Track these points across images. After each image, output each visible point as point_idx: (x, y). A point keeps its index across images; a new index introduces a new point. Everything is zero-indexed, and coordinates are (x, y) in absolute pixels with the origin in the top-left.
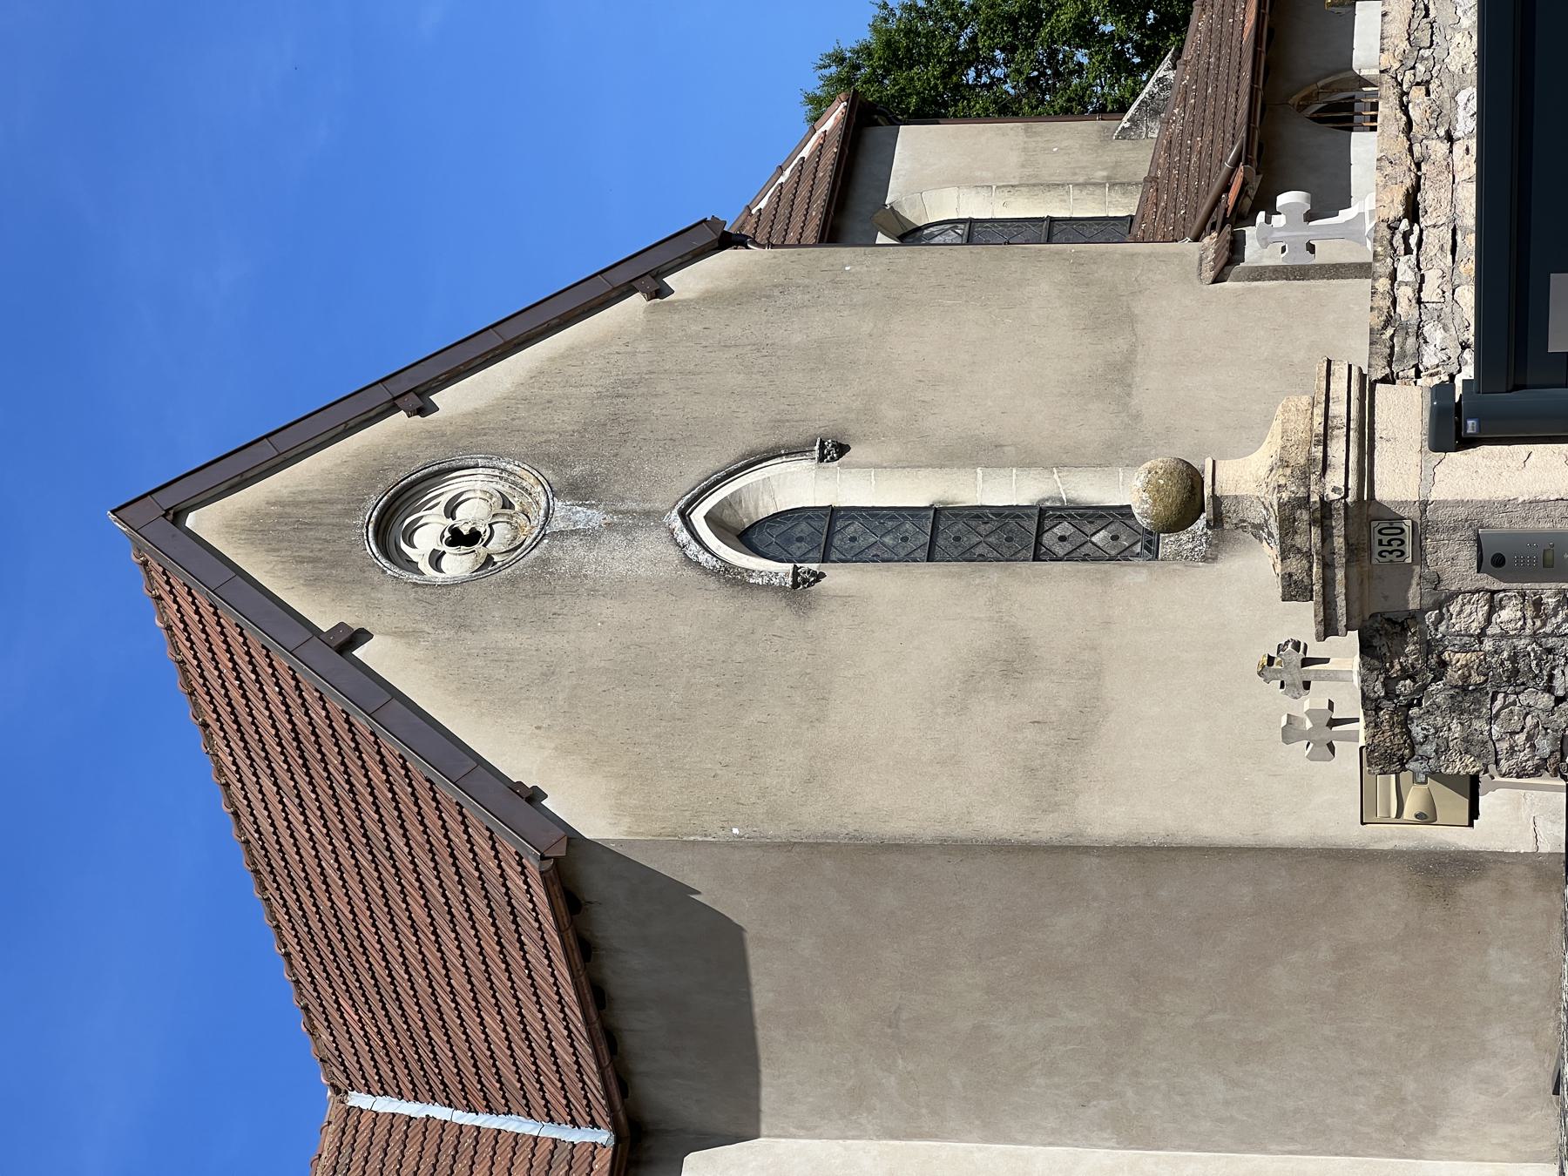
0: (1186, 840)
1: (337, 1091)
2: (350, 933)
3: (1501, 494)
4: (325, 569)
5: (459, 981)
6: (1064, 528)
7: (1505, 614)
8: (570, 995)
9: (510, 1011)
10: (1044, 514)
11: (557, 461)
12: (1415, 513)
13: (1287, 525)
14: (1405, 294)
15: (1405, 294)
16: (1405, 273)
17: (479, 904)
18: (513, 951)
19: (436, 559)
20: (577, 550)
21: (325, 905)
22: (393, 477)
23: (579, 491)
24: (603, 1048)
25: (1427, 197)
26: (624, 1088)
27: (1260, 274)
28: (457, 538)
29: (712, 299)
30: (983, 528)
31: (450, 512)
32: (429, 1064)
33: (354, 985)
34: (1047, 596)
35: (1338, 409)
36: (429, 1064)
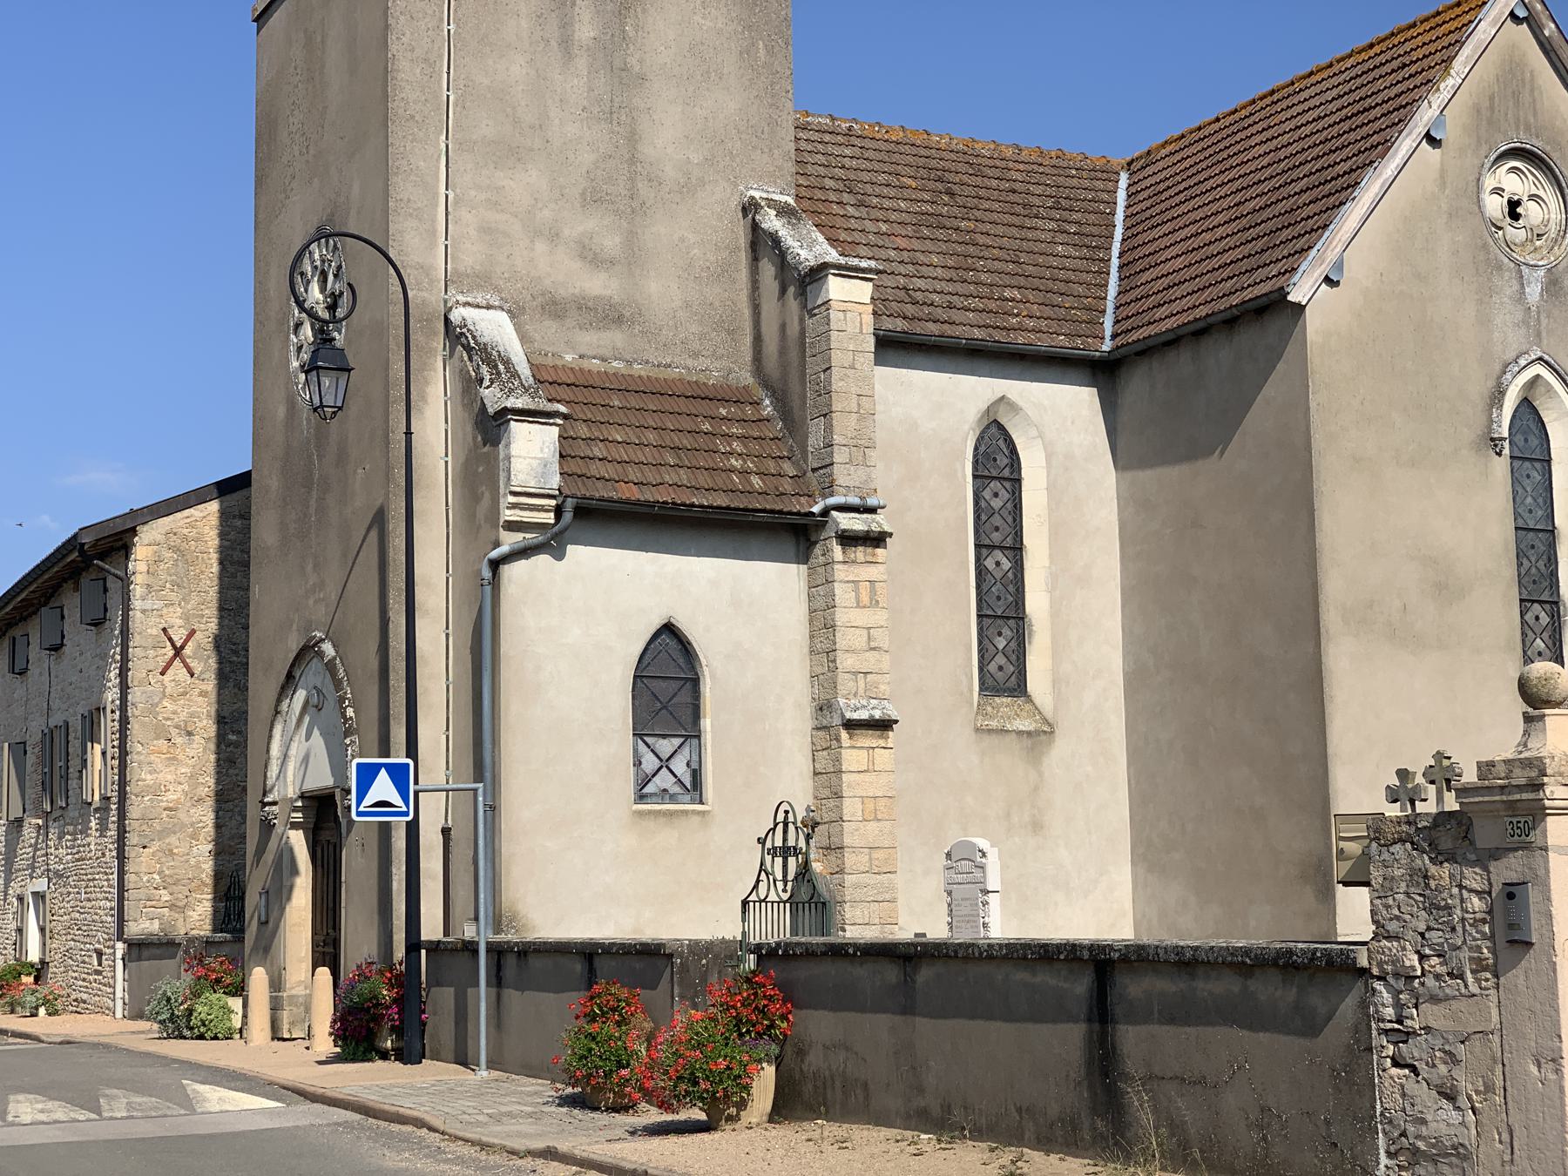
0: (1330, 709)
1: (1129, 164)
3: (1554, 896)
4: (1486, 115)
5: (1207, 237)
6: (1545, 619)
7: (1475, 900)
8: (1202, 312)
9: (1186, 274)
12: (1539, 843)
13: (1528, 763)
17: (1260, 244)
19: (1498, 191)
20: (1511, 288)
22: (1555, 156)
23: (1552, 284)
26: (1141, 354)
28: (1513, 207)
30: (1541, 564)
31: (1533, 197)
32: (1149, 224)
33: (1200, 167)
34: (1496, 609)
36: (1149, 224)
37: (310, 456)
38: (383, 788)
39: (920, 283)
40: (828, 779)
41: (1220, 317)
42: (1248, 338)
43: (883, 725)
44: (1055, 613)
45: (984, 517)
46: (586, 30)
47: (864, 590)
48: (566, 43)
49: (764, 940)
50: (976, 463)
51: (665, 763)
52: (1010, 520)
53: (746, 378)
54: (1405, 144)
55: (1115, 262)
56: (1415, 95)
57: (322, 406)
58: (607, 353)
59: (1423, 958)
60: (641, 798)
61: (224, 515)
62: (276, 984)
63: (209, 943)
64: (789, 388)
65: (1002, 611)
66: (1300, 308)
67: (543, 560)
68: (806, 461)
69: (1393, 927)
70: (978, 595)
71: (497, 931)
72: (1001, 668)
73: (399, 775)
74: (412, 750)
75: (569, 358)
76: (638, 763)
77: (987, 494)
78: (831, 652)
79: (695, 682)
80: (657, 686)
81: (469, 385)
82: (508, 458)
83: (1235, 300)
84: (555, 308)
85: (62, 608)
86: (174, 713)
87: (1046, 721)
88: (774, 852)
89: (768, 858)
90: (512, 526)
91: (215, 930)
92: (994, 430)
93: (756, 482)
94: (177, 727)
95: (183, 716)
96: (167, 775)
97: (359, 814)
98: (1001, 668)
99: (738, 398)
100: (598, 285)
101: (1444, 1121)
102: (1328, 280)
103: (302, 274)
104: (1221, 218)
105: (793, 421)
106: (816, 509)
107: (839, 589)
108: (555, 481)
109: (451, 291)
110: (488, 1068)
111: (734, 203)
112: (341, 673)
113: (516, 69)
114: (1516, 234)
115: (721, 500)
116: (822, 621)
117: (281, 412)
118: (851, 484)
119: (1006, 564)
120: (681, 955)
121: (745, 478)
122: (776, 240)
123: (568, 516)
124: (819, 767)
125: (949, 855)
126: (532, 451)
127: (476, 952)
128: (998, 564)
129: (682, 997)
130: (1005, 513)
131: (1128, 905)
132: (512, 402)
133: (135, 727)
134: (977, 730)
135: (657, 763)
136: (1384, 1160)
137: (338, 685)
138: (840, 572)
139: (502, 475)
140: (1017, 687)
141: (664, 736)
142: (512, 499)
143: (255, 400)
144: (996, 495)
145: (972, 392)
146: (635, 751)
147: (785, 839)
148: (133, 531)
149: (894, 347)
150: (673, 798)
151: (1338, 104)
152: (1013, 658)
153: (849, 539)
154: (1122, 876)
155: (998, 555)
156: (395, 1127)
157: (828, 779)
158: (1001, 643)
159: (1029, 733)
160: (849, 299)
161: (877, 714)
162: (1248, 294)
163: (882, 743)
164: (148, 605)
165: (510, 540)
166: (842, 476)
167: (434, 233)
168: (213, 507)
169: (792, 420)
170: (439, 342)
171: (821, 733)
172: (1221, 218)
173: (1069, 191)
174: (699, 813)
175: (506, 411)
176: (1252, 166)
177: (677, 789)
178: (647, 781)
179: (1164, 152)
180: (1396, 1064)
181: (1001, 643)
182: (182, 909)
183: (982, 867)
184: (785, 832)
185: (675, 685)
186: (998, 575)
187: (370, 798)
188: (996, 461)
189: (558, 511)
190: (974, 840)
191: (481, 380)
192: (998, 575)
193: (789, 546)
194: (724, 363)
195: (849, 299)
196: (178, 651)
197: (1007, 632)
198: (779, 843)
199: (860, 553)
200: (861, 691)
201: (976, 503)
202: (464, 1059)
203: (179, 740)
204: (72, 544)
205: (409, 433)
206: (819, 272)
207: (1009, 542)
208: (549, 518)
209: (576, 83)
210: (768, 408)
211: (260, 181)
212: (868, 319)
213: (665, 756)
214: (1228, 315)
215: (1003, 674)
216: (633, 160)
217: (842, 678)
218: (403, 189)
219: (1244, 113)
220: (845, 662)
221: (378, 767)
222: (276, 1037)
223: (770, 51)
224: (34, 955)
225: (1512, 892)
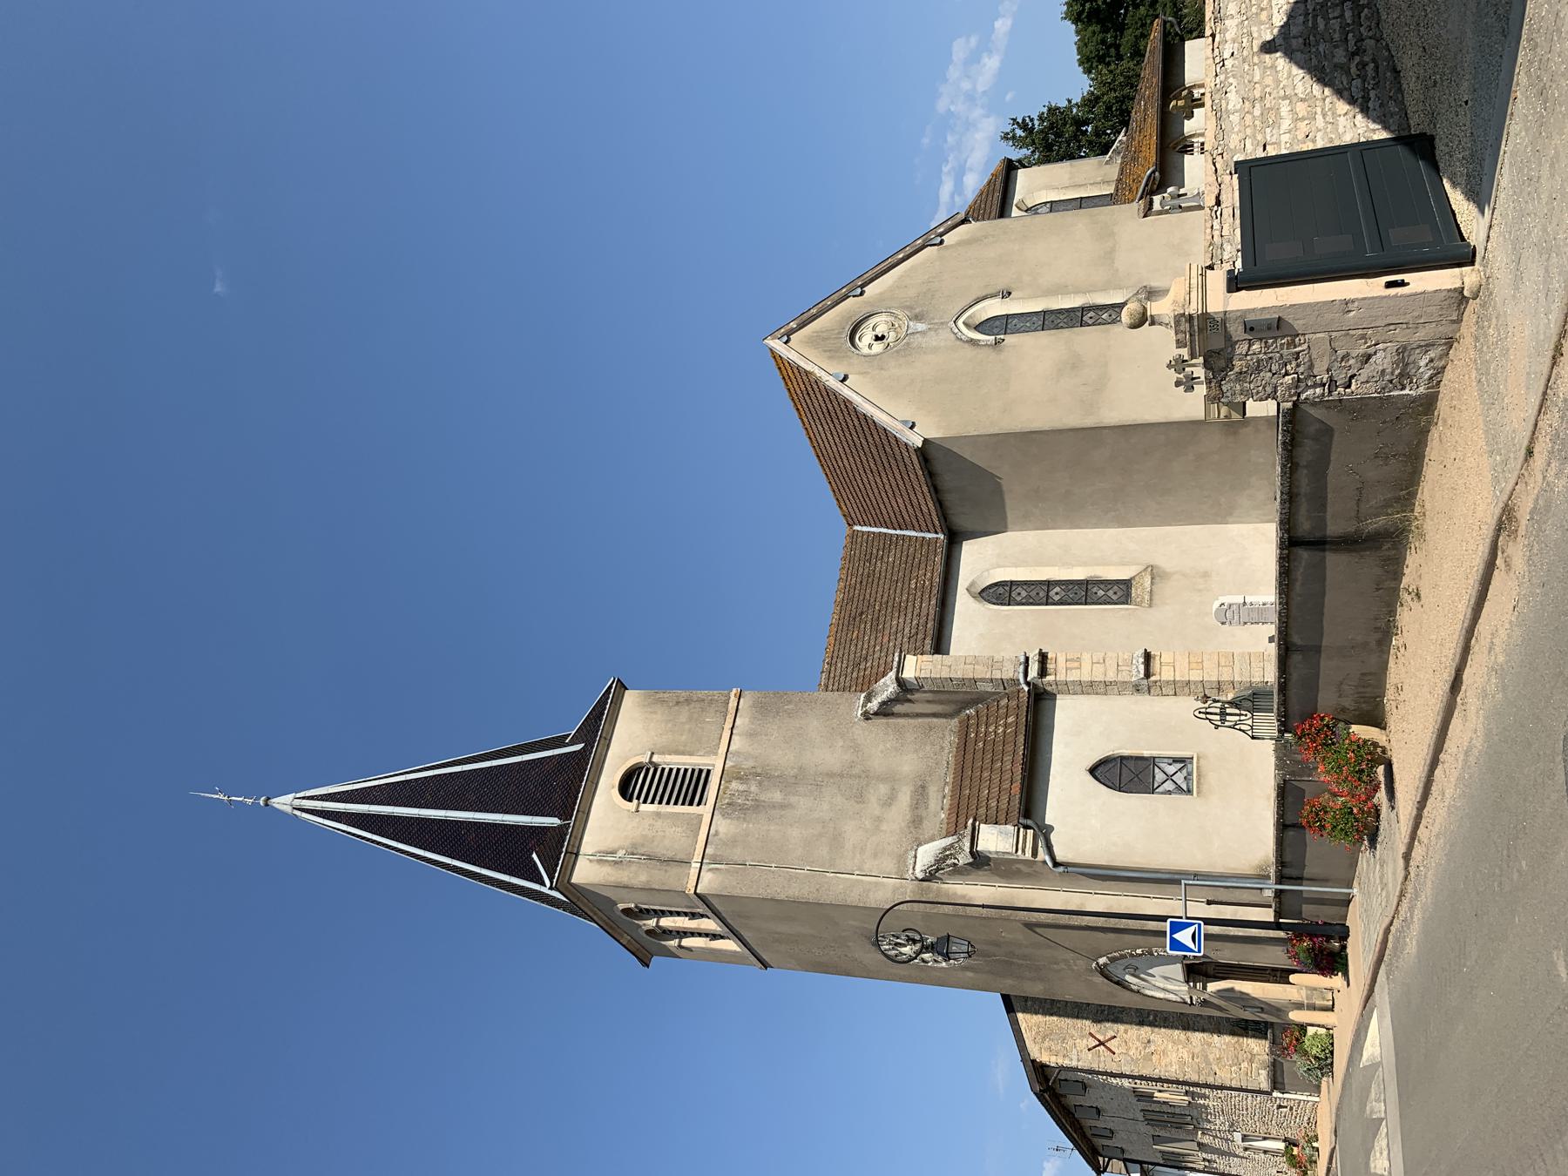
4: (833, 353)
6: (1091, 314)
8: (925, 489)
10: (1084, 310)
11: (910, 308)
13: (1177, 323)
14: (1216, 233)
15: (1216, 233)
16: (1217, 226)
19: (870, 346)
20: (919, 339)
23: (917, 318)
25: (1223, 198)
27: (1159, 213)
28: (878, 338)
29: (960, 244)
34: (1086, 339)
35: (1194, 281)
38: (1184, 937)
40: (1178, 688)
42: (939, 466)
43: (1148, 657)
44: (1085, 564)
46: (777, 796)
48: (783, 806)
51: (1169, 777)
53: (955, 722)
54: (846, 392)
59: (1287, 374)
60: (1189, 792)
62: (1299, 1006)
63: (1273, 1042)
64: (960, 700)
65: (1083, 592)
66: (926, 441)
67: (1053, 837)
69: (1269, 389)
71: (1268, 877)
73: (1177, 927)
74: (1163, 919)
76: (1169, 792)
79: (1123, 758)
80: (1125, 779)
81: (957, 871)
84: (916, 822)
90: (1035, 854)
93: (1010, 720)
96: (1173, 1057)
99: (965, 728)
100: (905, 797)
101: (1383, 360)
108: (1010, 828)
111: (863, 724)
113: (795, 833)
114: (892, 337)
115: (1021, 739)
117: (970, 974)
119: (1057, 589)
121: (1008, 726)
122: (883, 703)
123: (1029, 822)
126: (995, 839)
132: (967, 849)
133: (1144, 1072)
136: (1406, 392)
137: (1123, 957)
138: (1061, 677)
140: (1126, 584)
145: (965, 608)
148: (1033, 1061)
149: (940, 645)
150: (1190, 774)
153: (1043, 672)
154: (1234, 529)
155: (1052, 593)
156: (1390, 945)
157: (1178, 688)
158: (1101, 593)
162: (917, 466)
164: (1075, 1057)
165: (1042, 855)
166: (1008, 674)
167: (876, 884)
168: (1020, 1016)
169: (977, 699)
170: (934, 885)
173: (861, 555)
178: (1179, 788)
180: (1349, 386)
181: (1101, 593)
182: (1253, 1055)
187: (1191, 945)
188: (1000, 593)
189: (1027, 827)
193: (1046, 704)
194: (947, 733)
195: (914, 668)
196: (1101, 1043)
199: (1050, 666)
202: (1347, 902)
204: (1040, 1096)
205: (983, 906)
208: (1030, 832)
209: (802, 803)
212: (925, 657)
215: (1120, 592)
216: (841, 776)
217: (1120, 678)
218: (853, 898)
220: (1111, 676)
221: (1172, 940)
222: (1331, 1009)
223: (790, 702)
224: (1281, 1146)
225: (1250, 328)
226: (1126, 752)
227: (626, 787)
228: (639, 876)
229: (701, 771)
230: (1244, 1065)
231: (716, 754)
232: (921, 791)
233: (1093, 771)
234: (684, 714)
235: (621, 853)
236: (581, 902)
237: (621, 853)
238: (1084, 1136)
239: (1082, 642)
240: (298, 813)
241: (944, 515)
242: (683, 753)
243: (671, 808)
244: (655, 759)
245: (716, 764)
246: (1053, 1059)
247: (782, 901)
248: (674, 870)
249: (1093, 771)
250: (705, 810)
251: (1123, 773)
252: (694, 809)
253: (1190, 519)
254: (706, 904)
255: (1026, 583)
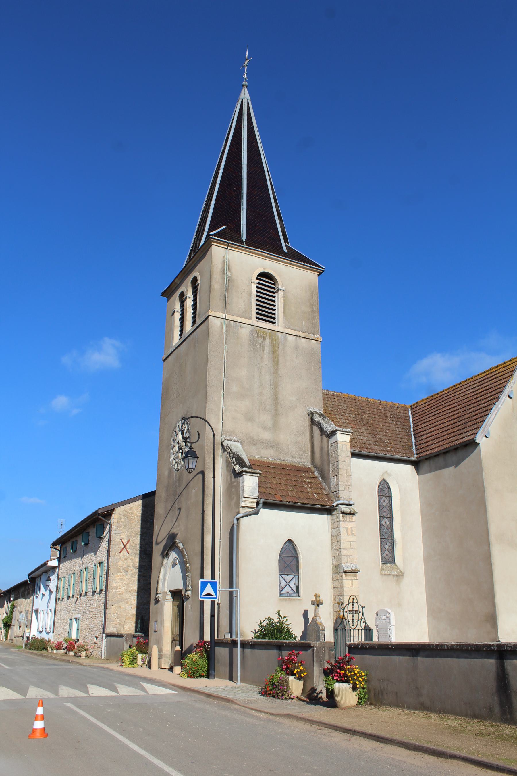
1: (411, 406)
2: (447, 404)
5: (443, 425)
18: (452, 435)
21: (451, 399)
24: (435, 454)
37: (176, 486)
38: (208, 589)
39: (361, 438)
41: (454, 448)
42: (460, 453)
43: (356, 572)
45: (381, 508)
47: (349, 529)
49: (352, 642)
50: (378, 491)
51: (288, 584)
52: (389, 509)
53: (308, 464)
54: (504, 397)
55: (412, 433)
56: (504, 384)
57: (189, 468)
58: (268, 456)
61: (144, 506)
62: (160, 651)
63: (134, 637)
64: (323, 467)
65: (387, 537)
66: (478, 444)
68: (329, 489)
70: (380, 532)
72: (387, 555)
73: (214, 585)
74: (213, 577)
75: (257, 457)
77: (382, 501)
78: (339, 549)
79: (297, 558)
81: (228, 464)
82: (243, 486)
83: (458, 442)
84: (253, 442)
85: (89, 533)
86: (123, 565)
87: (400, 571)
88: (358, 612)
89: (346, 615)
91: (136, 632)
92: (383, 481)
93: (316, 496)
94: (123, 569)
95: (125, 566)
96: (119, 584)
97: (201, 598)
98: (387, 555)
99: (308, 471)
100: (266, 436)
102: (486, 436)
103: (175, 432)
104: (446, 420)
105: (325, 478)
106: (335, 504)
107: (341, 529)
108: (257, 494)
109: (224, 436)
110: (241, 682)
111: (306, 413)
112: (185, 553)
116: (336, 540)
117: (167, 473)
118: (345, 497)
119: (388, 523)
120: (316, 647)
123: (261, 505)
124: (335, 586)
125: (377, 614)
126: (250, 484)
127: (237, 643)
128: (385, 522)
129: (317, 661)
130: (387, 507)
131: (427, 630)
132: (244, 469)
134: (381, 574)
135: (285, 584)
138: (342, 524)
139: (241, 492)
141: (288, 575)
142: (244, 499)
143: (158, 469)
144: (385, 501)
146: (279, 580)
147: (353, 608)
148: (113, 510)
151: (478, 388)
152: (391, 552)
155: (385, 520)
158: (387, 547)
159: (396, 575)
160: (343, 439)
161: (354, 569)
163: (355, 578)
165: (243, 511)
166: (342, 494)
170: (219, 450)
171: (336, 575)
172: (446, 420)
174: (298, 600)
175: (243, 472)
176: (454, 405)
177: (292, 592)
178: (282, 589)
179: (422, 403)
181: (387, 547)
183: (389, 618)
184: (353, 605)
185: (291, 559)
186: (386, 526)
187: (205, 592)
188: (384, 490)
189: (258, 503)
190: (386, 609)
191: (234, 463)
192: (386, 526)
194: (303, 460)
195: (343, 439)
196: (125, 546)
197: (388, 543)
198: (350, 609)
200: (348, 562)
201: (379, 504)
202: (231, 678)
203: (123, 573)
204: (96, 513)
206: (333, 433)
207: (389, 516)
210: (316, 474)
211: (162, 406)
212: (349, 447)
213: (288, 581)
214: (456, 447)
215: (388, 557)
218: (210, 406)
219: (446, 392)
220: (344, 552)
224: (74, 637)
226: (301, 560)
227: (264, 275)
228: (217, 285)
229: (274, 318)
230: (118, 620)
231: (285, 327)
232: (272, 445)
233: (290, 541)
234: (307, 309)
235: (229, 274)
236: (199, 253)
237: (229, 274)
238: (72, 537)
239: (361, 535)
240: (240, 102)
241: (429, 458)
242: (284, 308)
243: (254, 302)
244: (281, 292)
245: (280, 326)
246: (116, 521)
247: (206, 364)
248: (221, 304)
249: (290, 541)
250: (254, 321)
251: (289, 559)
252: (254, 315)
253: (430, 596)
254: (201, 321)
255: (391, 505)
